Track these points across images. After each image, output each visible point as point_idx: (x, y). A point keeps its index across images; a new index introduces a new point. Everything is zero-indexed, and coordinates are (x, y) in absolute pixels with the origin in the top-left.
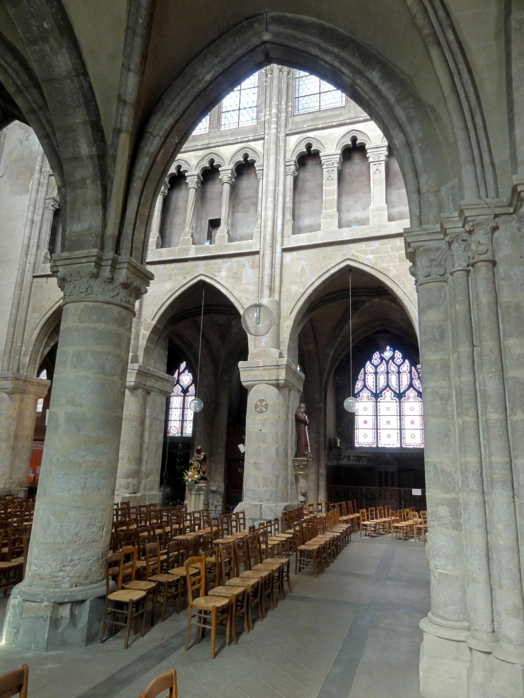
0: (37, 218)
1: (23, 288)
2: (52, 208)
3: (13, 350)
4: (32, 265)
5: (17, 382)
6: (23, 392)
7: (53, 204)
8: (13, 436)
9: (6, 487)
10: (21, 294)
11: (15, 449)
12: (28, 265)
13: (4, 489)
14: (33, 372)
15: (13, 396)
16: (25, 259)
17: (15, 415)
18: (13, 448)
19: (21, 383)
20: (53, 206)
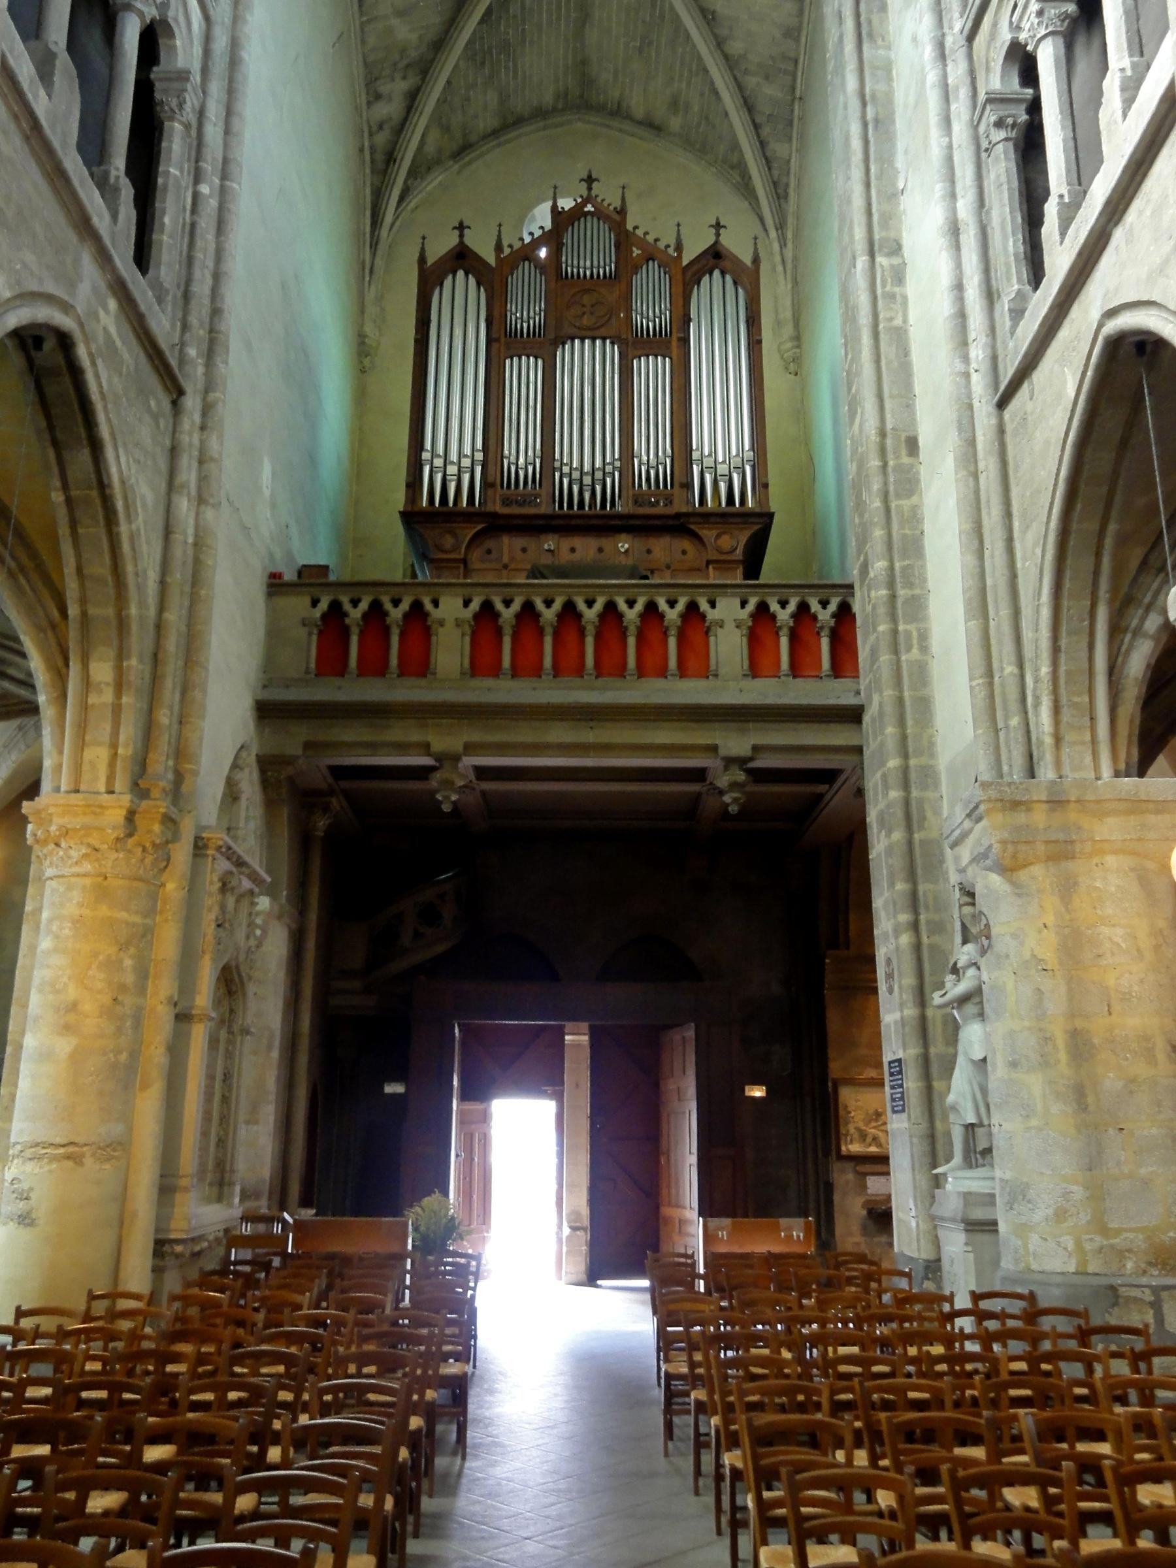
0: (965, 207)
1: (981, 465)
2: (1002, 134)
3: (998, 700)
4: (985, 367)
5: (1021, 818)
6: (1061, 852)
7: (993, 119)
8: (1061, 1040)
9: (1090, 1269)
10: (977, 492)
11: (1090, 1099)
12: (975, 378)
13: (1077, 1280)
14: (1088, 759)
15: (1023, 875)
16: (959, 366)
17: (1049, 955)
18: (1079, 1094)
19: (1039, 817)
20: (999, 124)
